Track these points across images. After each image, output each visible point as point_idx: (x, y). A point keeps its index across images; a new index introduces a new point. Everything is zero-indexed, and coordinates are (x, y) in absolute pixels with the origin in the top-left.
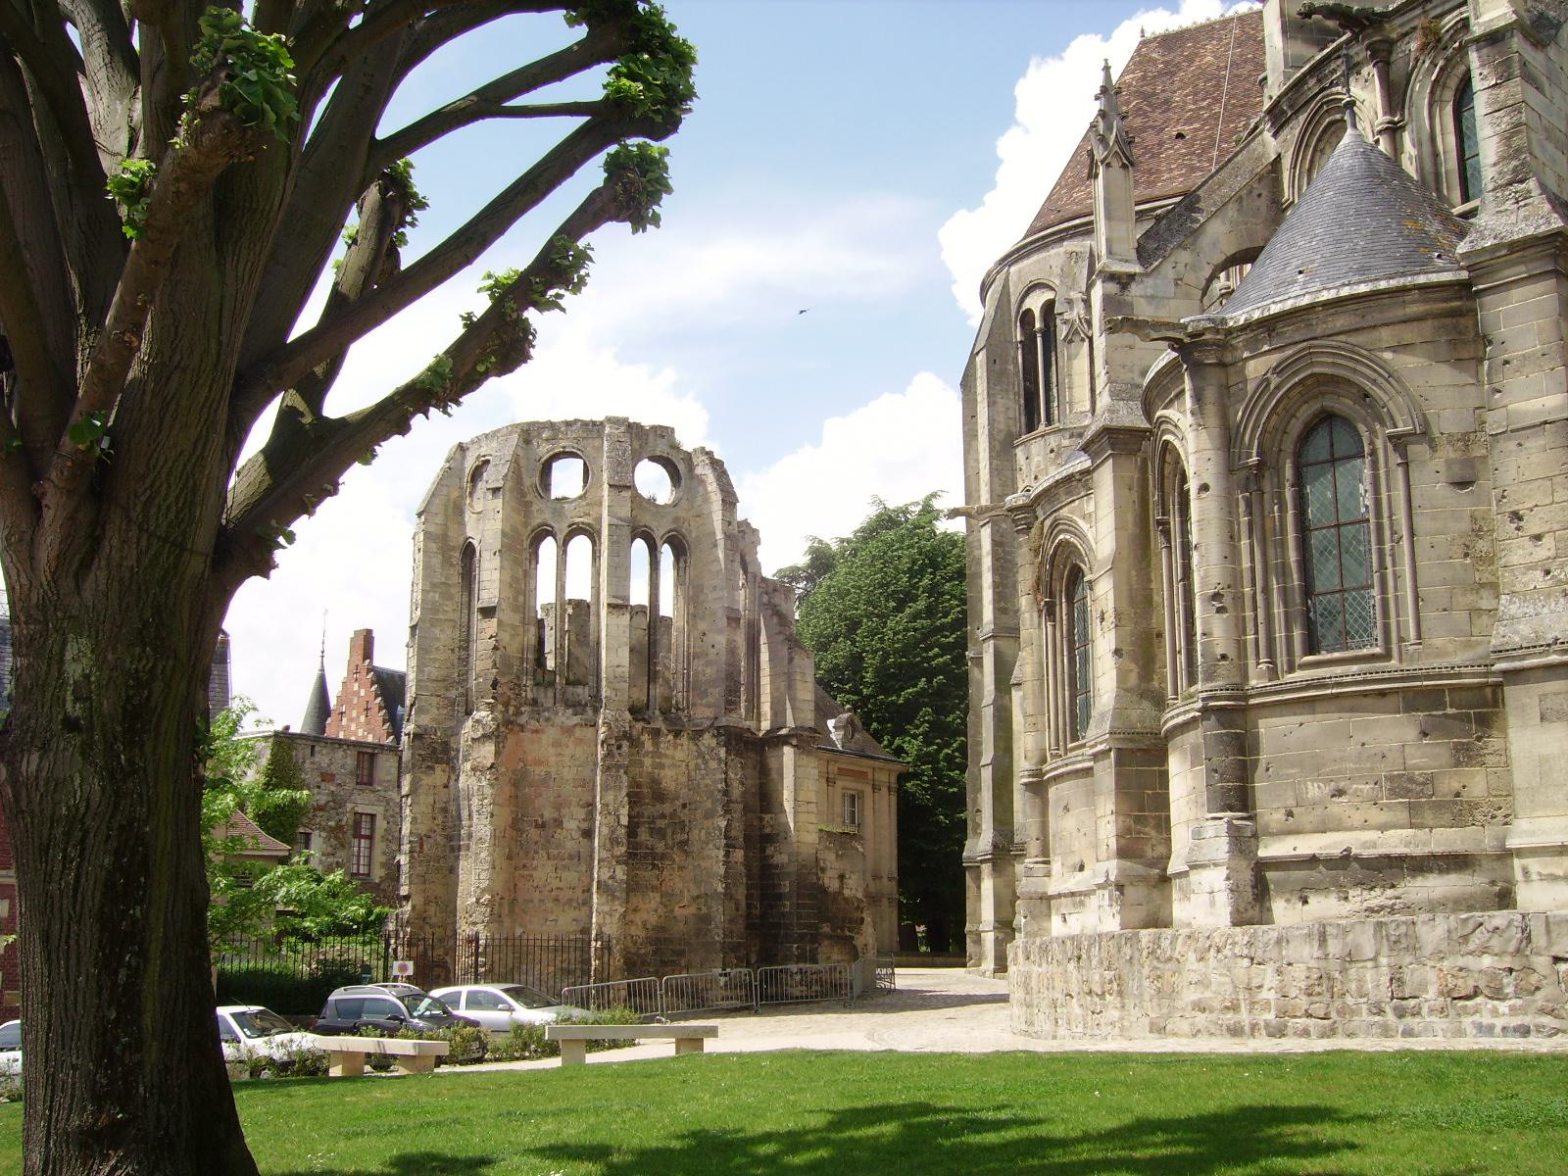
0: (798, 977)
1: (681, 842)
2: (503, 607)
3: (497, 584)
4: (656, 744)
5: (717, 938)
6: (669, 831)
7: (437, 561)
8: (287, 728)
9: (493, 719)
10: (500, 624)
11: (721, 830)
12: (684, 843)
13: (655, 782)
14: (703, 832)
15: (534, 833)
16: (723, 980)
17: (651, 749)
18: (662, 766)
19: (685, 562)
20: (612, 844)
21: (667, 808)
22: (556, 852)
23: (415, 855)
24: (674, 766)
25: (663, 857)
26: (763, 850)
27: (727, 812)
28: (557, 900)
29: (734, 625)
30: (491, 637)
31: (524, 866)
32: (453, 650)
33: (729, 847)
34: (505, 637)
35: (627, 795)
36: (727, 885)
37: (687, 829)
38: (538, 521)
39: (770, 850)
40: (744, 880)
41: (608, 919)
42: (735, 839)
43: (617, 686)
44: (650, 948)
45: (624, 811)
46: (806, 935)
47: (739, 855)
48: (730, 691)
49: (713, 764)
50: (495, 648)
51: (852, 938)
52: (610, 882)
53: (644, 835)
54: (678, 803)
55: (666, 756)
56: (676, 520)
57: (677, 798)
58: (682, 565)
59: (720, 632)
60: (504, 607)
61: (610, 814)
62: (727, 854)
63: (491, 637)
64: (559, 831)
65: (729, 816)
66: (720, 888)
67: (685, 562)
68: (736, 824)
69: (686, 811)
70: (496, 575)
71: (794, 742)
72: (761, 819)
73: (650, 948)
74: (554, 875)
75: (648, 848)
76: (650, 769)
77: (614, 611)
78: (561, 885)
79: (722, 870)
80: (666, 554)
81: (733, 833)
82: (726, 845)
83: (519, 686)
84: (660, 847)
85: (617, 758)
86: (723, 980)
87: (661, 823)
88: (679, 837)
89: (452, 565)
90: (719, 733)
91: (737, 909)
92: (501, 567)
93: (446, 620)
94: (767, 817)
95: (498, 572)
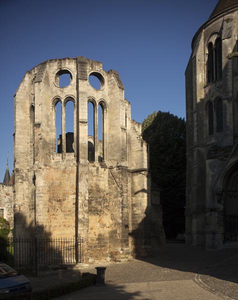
6: (102, 203)
13: (97, 186)
14: (114, 203)
18: (100, 180)
19: (106, 110)
22: (64, 210)
27: (122, 196)
30: (39, 135)
41: (82, 232)
44: (97, 242)
45: (87, 195)
52: (83, 219)
53: (93, 203)
54: (105, 193)
55: (101, 177)
58: (105, 111)
63: (39, 135)
66: (120, 221)
67: (106, 110)
69: (108, 196)
72: (132, 199)
73: (97, 242)
84: (99, 208)
87: (100, 200)
88: (106, 204)
89: (26, 113)
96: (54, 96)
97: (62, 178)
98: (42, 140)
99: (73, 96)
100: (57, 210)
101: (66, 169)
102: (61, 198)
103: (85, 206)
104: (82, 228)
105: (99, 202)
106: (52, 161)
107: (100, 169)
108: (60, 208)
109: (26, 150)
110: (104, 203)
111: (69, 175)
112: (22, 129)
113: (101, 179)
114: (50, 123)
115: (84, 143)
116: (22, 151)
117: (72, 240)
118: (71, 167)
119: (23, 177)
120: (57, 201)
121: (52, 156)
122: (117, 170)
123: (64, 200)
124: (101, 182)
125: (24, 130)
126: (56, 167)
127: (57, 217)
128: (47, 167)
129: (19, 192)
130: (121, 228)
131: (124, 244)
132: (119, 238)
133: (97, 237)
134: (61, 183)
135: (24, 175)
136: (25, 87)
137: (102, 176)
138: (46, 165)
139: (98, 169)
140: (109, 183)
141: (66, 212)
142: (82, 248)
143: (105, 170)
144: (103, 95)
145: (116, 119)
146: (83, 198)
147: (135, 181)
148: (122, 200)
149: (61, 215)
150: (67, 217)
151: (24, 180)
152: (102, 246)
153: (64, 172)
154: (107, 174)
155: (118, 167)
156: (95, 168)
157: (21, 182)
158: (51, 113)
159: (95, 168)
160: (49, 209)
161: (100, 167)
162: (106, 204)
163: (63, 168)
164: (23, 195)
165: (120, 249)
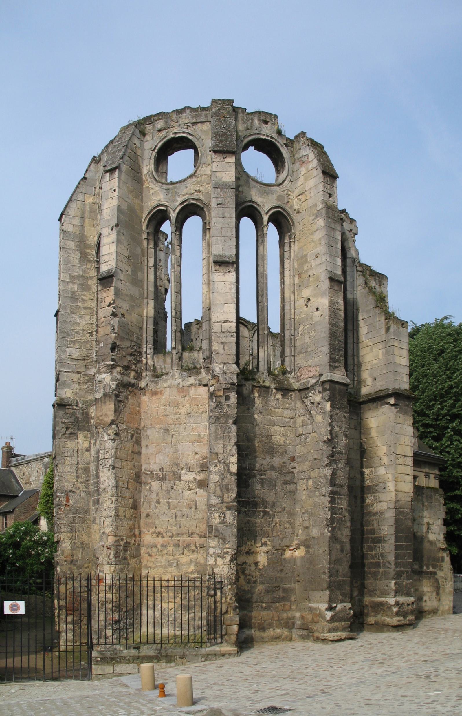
2: (122, 277)
3: (114, 256)
4: (266, 402)
6: (279, 484)
7: (75, 257)
9: (112, 379)
10: (118, 293)
14: (310, 482)
15: (155, 485)
20: (222, 490)
21: (277, 461)
33: (334, 496)
36: (334, 529)
38: (155, 204)
40: (349, 524)
41: (220, 561)
42: (341, 486)
43: (224, 340)
48: (334, 350)
49: (319, 418)
50: (114, 315)
59: (323, 295)
61: (220, 462)
62: (332, 501)
64: (177, 483)
65: (334, 466)
68: (340, 473)
80: (272, 231)
81: (338, 481)
82: (332, 493)
83: (141, 353)
85: (226, 409)
86: (329, 615)
90: (325, 390)
91: (342, 551)
93: (85, 308)
131: (338, 592)
142: (219, 605)
148: (334, 474)
155: (323, 383)
165: (323, 606)
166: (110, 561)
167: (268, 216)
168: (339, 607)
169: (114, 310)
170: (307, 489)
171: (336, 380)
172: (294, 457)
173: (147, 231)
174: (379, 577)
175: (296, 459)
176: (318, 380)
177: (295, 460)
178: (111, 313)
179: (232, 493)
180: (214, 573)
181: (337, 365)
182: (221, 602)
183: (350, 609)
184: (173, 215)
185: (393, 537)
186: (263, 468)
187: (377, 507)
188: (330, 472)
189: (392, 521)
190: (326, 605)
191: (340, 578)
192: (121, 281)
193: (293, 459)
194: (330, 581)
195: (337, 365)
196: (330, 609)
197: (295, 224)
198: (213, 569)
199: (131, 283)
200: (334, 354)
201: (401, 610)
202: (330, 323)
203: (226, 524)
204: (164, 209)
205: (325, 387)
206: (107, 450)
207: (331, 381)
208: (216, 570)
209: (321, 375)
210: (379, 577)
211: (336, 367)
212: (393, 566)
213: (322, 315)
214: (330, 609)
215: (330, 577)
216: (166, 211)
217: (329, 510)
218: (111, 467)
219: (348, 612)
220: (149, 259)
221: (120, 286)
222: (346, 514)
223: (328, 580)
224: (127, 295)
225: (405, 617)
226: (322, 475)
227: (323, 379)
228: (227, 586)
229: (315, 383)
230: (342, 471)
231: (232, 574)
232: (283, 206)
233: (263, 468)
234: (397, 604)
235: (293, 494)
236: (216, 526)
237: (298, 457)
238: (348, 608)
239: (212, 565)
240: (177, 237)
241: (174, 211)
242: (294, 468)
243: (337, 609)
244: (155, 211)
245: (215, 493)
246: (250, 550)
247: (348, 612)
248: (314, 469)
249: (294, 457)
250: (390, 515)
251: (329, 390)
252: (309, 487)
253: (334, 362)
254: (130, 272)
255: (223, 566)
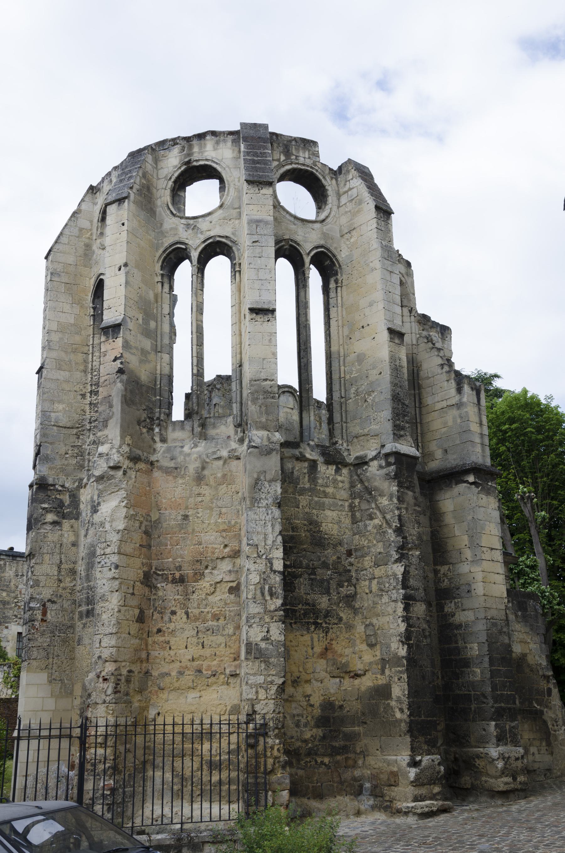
0: (500, 765)
1: (347, 596)
5: (398, 715)
8: (12, 549)
10: (126, 345)
11: (398, 579)
12: (350, 599)
16: (413, 773)
17: (307, 486)
18: (322, 507)
19: (336, 282)
22: (196, 611)
23: (37, 624)
24: (335, 505)
25: (328, 614)
26: (440, 607)
28: (200, 671)
29: (397, 341)
31: (159, 631)
32: (83, 396)
33: (408, 601)
34: (133, 360)
35: (280, 533)
37: (354, 581)
39: (449, 607)
41: (262, 695)
45: (279, 553)
46: (504, 709)
47: (420, 609)
48: (398, 415)
50: (121, 371)
51: (542, 712)
55: (326, 495)
56: (325, 235)
57: (340, 543)
58: (332, 285)
60: (131, 325)
61: (259, 557)
66: (403, 651)
67: (336, 282)
68: (413, 571)
70: (122, 291)
71: (471, 479)
72: (436, 572)
73: (319, 732)
74: (195, 640)
75: (308, 604)
76: (307, 510)
77: (258, 317)
78: (202, 652)
79: (403, 627)
81: (412, 582)
84: (323, 602)
86: (413, 773)
88: (345, 590)
91: (423, 678)
92: (127, 283)
94: (443, 569)
95: (123, 286)
96: (166, 244)
97: (191, 500)
98: (124, 377)
99: (227, 237)
100: (174, 613)
101: (203, 468)
102: (188, 571)
103: (272, 594)
104: (260, 679)
105: (322, 581)
106: (159, 445)
107: (322, 468)
108: (185, 607)
109: (76, 417)
110: (340, 585)
111: (216, 489)
112: (66, 352)
113: (326, 500)
114: (153, 324)
115: (263, 376)
116: (64, 421)
117: (225, 728)
118: (221, 462)
119: (61, 504)
120: (174, 581)
121: (157, 430)
122: (381, 467)
123: (199, 576)
124: (328, 513)
125: (72, 356)
126: (172, 464)
127: (173, 641)
128: (141, 466)
129: (47, 557)
130: (405, 676)
131: (422, 739)
132: (398, 715)
133: (317, 712)
134: (186, 517)
135: (66, 499)
136: (81, 230)
137: (330, 490)
138: (135, 459)
139: (313, 465)
140: (353, 516)
141: (205, 621)
143: (338, 471)
144: (325, 235)
145: (371, 305)
146: (262, 566)
147: (444, 509)
148: (406, 574)
149: (187, 633)
150: (209, 639)
151: (64, 516)
152: (335, 751)
153: (199, 479)
154: (347, 485)
155: (387, 455)
156: (306, 464)
157: (55, 523)
158: (156, 296)
159: (306, 464)
160: (142, 612)
161: (320, 459)
162: (345, 590)
163: (193, 466)
164: (59, 567)
165: (404, 758)
166: (108, 699)
167: (310, 257)
168: (426, 760)
169: (121, 366)
170: (371, 592)
171: (402, 452)
172: (351, 550)
173: (162, 272)
174: (471, 716)
175: (353, 552)
176: (380, 453)
177: (352, 555)
178: (117, 369)
179: (277, 598)
180: (254, 712)
181: (402, 433)
182: (265, 756)
183: (439, 764)
184: (195, 255)
185: (486, 659)
186: (313, 564)
187: (461, 617)
188: (402, 569)
189: (483, 638)
190: (407, 759)
191: (423, 718)
192: (130, 330)
193: (349, 553)
194: (411, 720)
195: (402, 433)
196: (414, 764)
197: (343, 267)
198: (253, 706)
199: (142, 334)
200: (399, 420)
201: (507, 766)
202: (391, 383)
203: (270, 641)
204: (183, 247)
205: (389, 460)
206: (109, 543)
207: (397, 454)
208: (257, 708)
209: (383, 446)
210: (471, 716)
211: (402, 436)
212: (491, 702)
213: (381, 373)
214: (414, 764)
215: (409, 716)
216: (186, 249)
217: (403, 621)
218: (113, 566)
219: (437, 768)
220: (164, 306)
221: (130, 338)
222: (425, 626)
223: (408, 720)
224: (136, 348)
225: (515, 779)
226: (390, 573)
227: (387, 450)
228: (273, 730)
229: (376, 456)
230: (416, 569)
231: (279, 713)
232: (328, 246)
233: (313, 564)
234: (502, 756)
235: (351, 599)
236: (256, 644)
237: (356, 550)
238: (436, 763)
239: (252, 699)
240: (199, 280)
241: (196, 249)
242: (351, 564)
243: (423, 764)
244: (170, 249)
245: (255, 598)
246: (298, 678)
247: (437, 768)
248: (378, 566)
249: (351, 550)
250: (481, 627)
251: (394, 464)
252: (374, 591)
253: (398, 430)
254: (140, 321)
255: (266, 701)
